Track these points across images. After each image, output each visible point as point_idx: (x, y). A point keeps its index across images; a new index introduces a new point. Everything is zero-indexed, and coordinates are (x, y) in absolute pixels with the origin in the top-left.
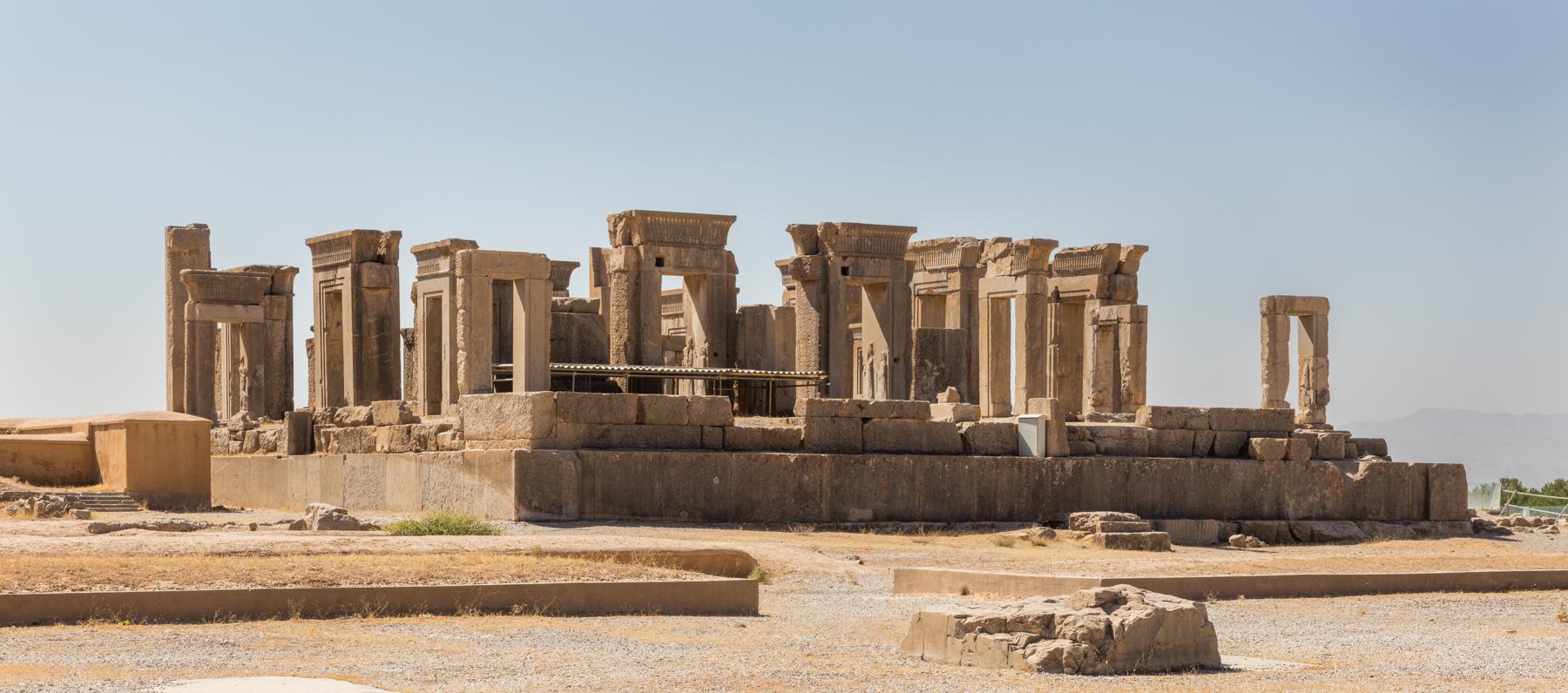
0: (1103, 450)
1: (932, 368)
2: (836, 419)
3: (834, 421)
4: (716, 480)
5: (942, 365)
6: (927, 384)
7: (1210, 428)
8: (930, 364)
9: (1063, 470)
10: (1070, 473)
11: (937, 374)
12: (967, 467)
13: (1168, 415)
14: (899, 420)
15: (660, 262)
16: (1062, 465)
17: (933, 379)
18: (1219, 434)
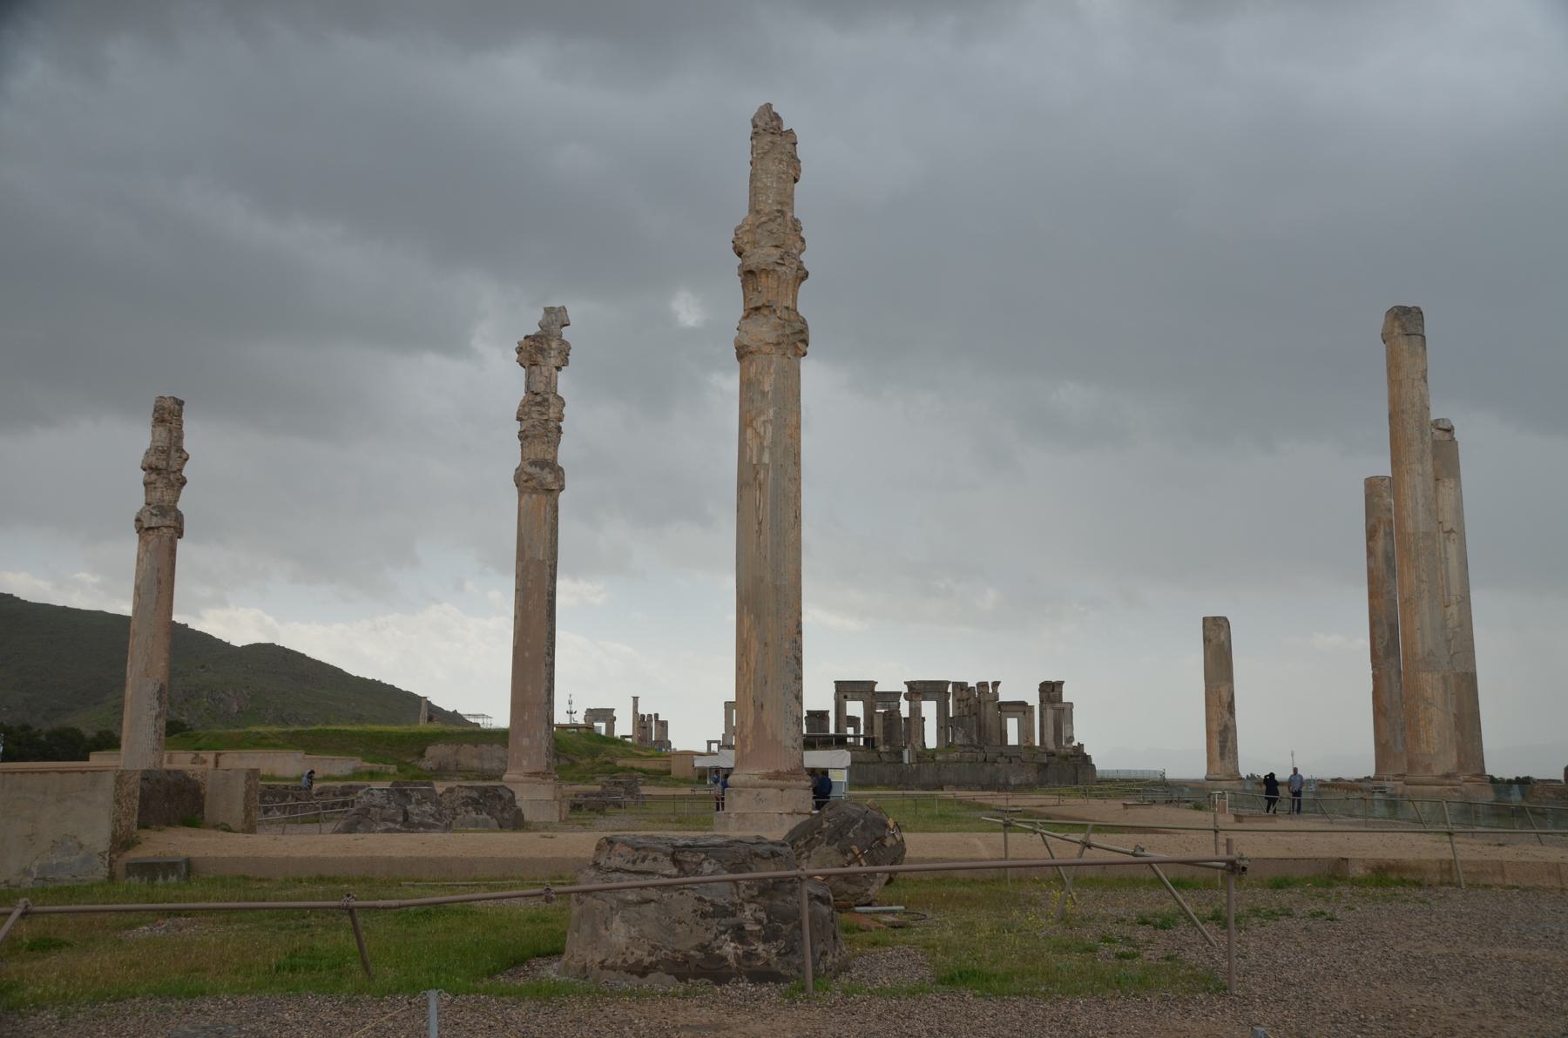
9: (912, 767)
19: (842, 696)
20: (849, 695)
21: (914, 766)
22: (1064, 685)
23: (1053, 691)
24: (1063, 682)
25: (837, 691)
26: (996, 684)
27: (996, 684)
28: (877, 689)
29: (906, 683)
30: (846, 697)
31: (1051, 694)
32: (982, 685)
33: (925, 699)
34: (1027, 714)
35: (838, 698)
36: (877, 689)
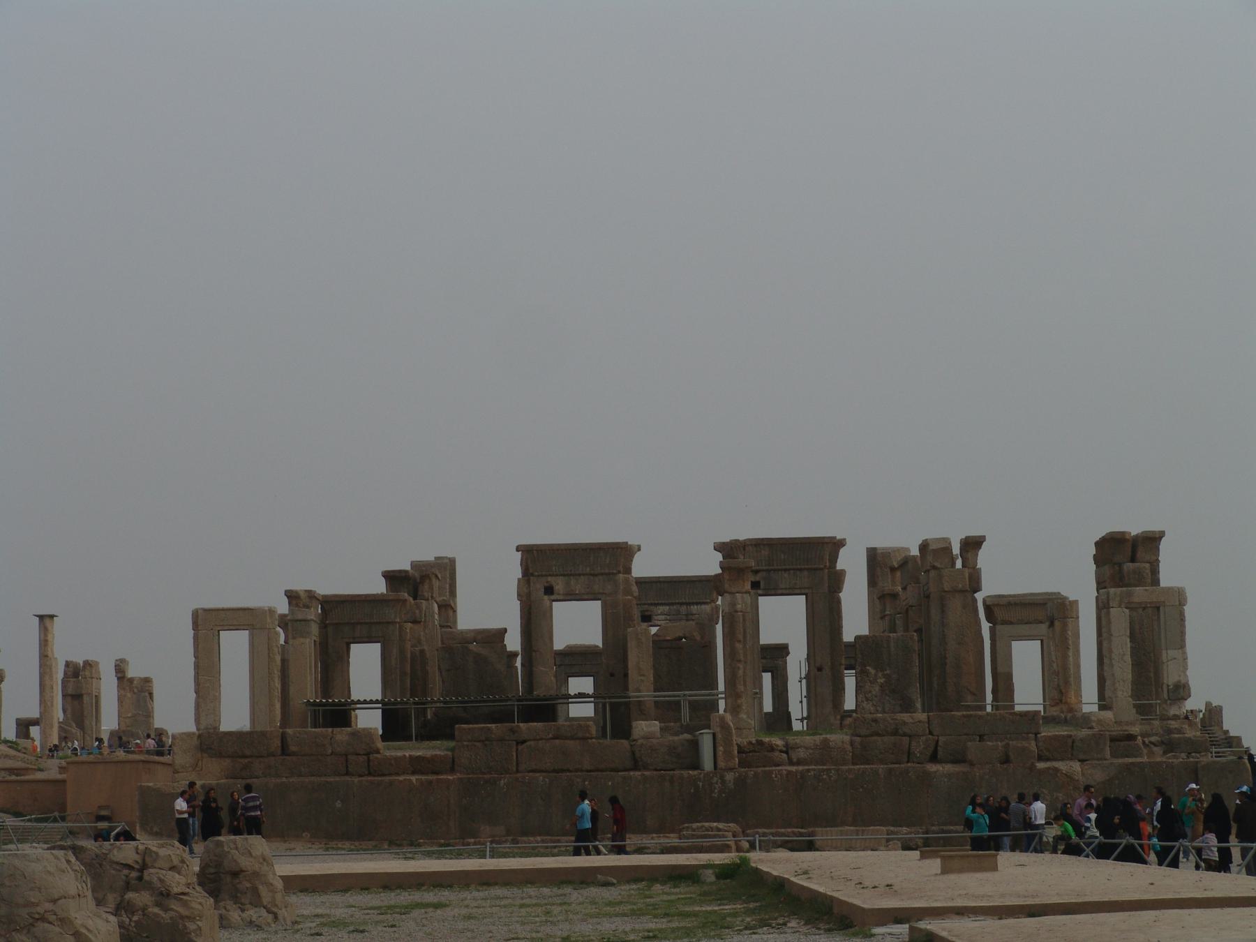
0: (795, 760)
1: (876, 675)
2: (487, 742)
3: (486, 745)
4: (338, 804)
5: (888, 672)
6: (870, 692)
7: (931, 733)
8: (873, 671)
9: (723, 782)
10: (731, 785)
11: (881, 681)
12: (610, 783)
13: (874, 724)
14: (557, 741)
15: (549, 590)
16: (722, 778)
17: (877, 688)
18: (942, 739)
19: (538, 587)
20: (559, 584)
21: (729, 777)
22: (1164, 545)
23: (1133, 560)
24: (1161, 535)
25: (527, 573)
26: (972, 545)
27: (972, 545)
28: (642, 567)
29: (720, 547)
30: (549, 590)
31: (1128, 566)
32: (934, 552)
33: (772, 591)
34: (1057, 623)
35: (529, 595)
36: (642, 567)
